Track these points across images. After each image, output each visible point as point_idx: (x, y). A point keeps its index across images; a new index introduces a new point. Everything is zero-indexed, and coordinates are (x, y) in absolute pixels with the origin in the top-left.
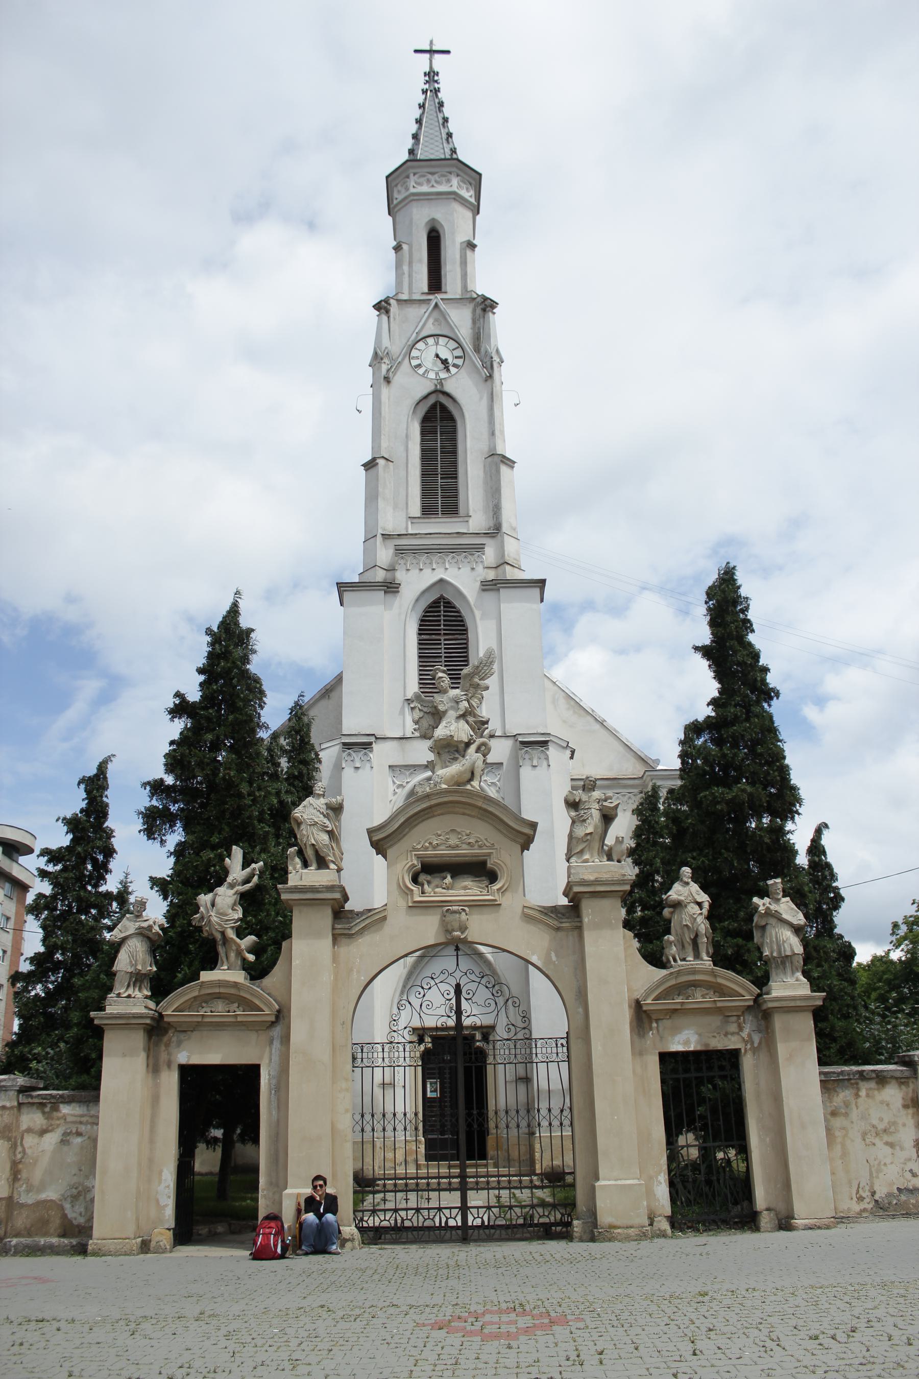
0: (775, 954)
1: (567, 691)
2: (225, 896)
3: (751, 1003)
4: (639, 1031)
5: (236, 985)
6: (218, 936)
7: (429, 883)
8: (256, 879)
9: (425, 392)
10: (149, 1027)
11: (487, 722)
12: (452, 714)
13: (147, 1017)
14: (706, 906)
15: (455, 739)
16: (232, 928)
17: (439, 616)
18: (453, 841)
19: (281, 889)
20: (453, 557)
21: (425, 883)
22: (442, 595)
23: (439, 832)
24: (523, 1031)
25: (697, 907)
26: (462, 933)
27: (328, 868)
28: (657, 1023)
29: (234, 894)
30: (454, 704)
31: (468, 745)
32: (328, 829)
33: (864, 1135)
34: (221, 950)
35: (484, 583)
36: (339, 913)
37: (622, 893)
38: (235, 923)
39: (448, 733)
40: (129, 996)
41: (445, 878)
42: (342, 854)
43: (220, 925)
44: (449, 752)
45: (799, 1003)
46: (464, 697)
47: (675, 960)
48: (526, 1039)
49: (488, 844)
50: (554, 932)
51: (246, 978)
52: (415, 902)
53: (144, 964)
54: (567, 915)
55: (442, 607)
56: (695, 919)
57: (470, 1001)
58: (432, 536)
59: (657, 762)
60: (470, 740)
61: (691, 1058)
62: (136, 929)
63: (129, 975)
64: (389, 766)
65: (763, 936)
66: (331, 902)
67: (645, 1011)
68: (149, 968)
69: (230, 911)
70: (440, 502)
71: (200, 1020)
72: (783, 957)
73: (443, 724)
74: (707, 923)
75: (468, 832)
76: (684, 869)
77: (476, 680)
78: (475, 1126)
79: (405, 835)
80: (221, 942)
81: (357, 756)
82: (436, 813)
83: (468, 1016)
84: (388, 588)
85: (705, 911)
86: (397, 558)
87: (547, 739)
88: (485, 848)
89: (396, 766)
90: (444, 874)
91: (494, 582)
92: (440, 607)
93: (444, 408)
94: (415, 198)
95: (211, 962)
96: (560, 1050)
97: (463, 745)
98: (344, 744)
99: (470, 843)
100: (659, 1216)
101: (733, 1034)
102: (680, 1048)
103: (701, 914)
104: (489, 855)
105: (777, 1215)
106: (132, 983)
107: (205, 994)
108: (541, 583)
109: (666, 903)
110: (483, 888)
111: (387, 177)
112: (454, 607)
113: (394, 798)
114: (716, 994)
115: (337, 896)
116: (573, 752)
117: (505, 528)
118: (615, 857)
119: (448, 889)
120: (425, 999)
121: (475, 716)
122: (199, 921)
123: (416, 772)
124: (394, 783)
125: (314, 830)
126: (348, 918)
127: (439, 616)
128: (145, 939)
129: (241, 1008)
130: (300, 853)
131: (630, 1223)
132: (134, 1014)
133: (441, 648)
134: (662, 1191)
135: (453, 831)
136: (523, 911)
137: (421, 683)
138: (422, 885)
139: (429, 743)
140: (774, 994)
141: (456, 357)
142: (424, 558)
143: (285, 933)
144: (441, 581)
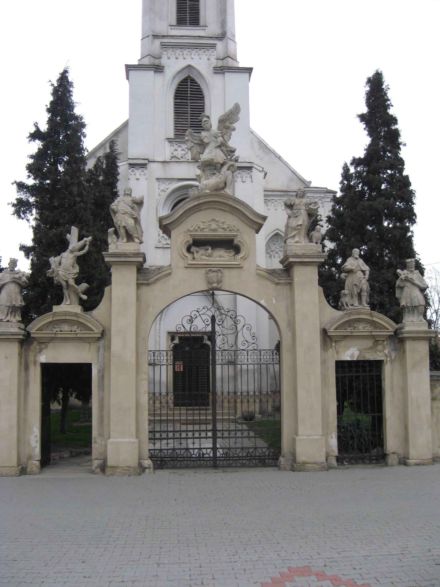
0: (409, 305)
1: (259, 138)
3: (392, 333)
4: (324, 348)
5: (76, 315)
6: (64, 284)
7: (197, 252)
8: (87, 247)
10: (21, 340)
11: (234, 151)
12: (212, 145)
13: (20, 335)
14: (368, 273)
15: (215, 161)
16: (73, 278)
17: (187, 88)
18: (214, 226)
19: (104, 254)
20: (197, 52)
21: (195, 253)
22: (189, 75)
23: (205, 221)
24: (253, 345)
25: (362, 274)
26: (218, 284)
27: (134, 241)
28: (335, 343)
29: (73, 257)
30: (214, 139)
31: (223, 165)
32: (134, 217)
34: (65, 292)
36: (140, 269)
37: (319, 263)
38: (74, 275)
39: (211, 157)
40: (8, 321)
41: (207, 250)
42: (143, 233)
43: (65, 276)
44: (210, 169)
45: (422, 335)
46: (220, 135)
47: (347, 305)
48: (255, 350)
49: (235, 229)
50: (274, 285)
51: (81, 310)
52: (189, 264)
53: (16, 300)
54: (282, 275)
55: (189, 83)
56: (361, 281)
57: (221, 326)
58: (184, 37)
59: (310, 182)
60: (224, 162)
61: (353, 364)
62: (11, 279)
63: (7, 308)
64: (157, 179)
65: (401, 293)
66: (137, 263)
67: (329, 336)
68: (20, 303)
69: (71, 268)
70: (188, 16)
71: (53, 336)
72: (413, 307)
73: (207, 151)
74: (367, 283)
75: (223, 221)
76: (355, 249)
77: (227, 124)
79: (183, 222)
80: (65, 287)
81: (138, 172)
82: (202, 208)
83: (219, 335)
84: (157, 69)
85: (367, 276)
86: (161, 50)
87: (252, 166)
88: (233, 231)
89: (161, 179)
90: (207, 247)
91: (222, 68)
92: (188, 82)
95: (59, 300)
96: (275, 357)
97: (219, 165)
98: (130, 164)
99: (224, 228)
100: (331, 456)
102: (349, 359)
103: (365, 278)
104: (236, 236)
105: (398, 456)
106: (9, 313)
107: (56, 320)
108: (249, 70)
109: (343, 270)
110: (231, 257)
112: (196, 83)
113: (159, 198)
114: (372, 327)
115: (141, 259)
116: (266, 174)
117: (229, 35)
118: (314, 241)
119: (209, 256)
120: (193, 324)
121: (226, 146)
122: (51, 274)
123: (172, 183)
124: (159, 189)
125: (126, 217)
126: (145, 273)
127: (187, 88)
128: (17, 285)
129: (79, 329)
130: (116, 233)
132: (12, 332)
133: (188, 108)
134: (334, 442)
135: (213, 220)
136: (256, 272)
137: (175, 129)
138: (193, 253)
139: (197, 164)
140: (407, 329)
142: (178, 51)
143: (106, 281)
144: (189, 66)
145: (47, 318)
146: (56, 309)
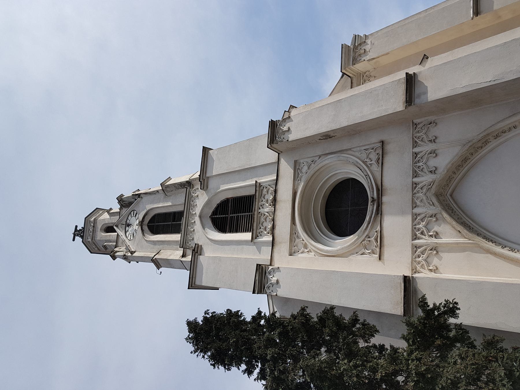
9: (140, 231)
35: (202, 188)
84: (197, 253)
93: (149, 222)
94: (94, 239)
111: (91, 253)
141: (134, 215)
144: (200, 217)
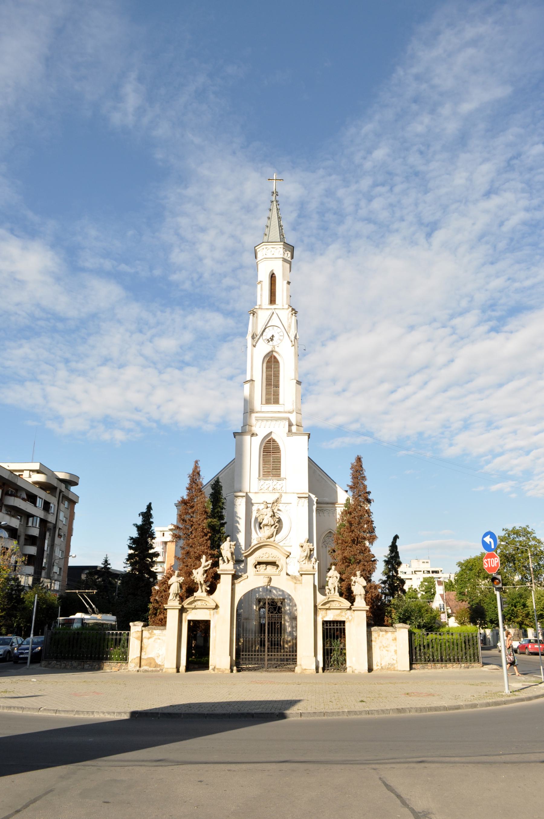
2: (201, 570)
3: (349, 608)
6: (199, 583)
14: (339, 578)
33: (380, 647)
78: (273, 639)
101: (344, 616)
130: (223, 559)
131: (310, 669)
145: (191, 599)
146: (195, 594)
